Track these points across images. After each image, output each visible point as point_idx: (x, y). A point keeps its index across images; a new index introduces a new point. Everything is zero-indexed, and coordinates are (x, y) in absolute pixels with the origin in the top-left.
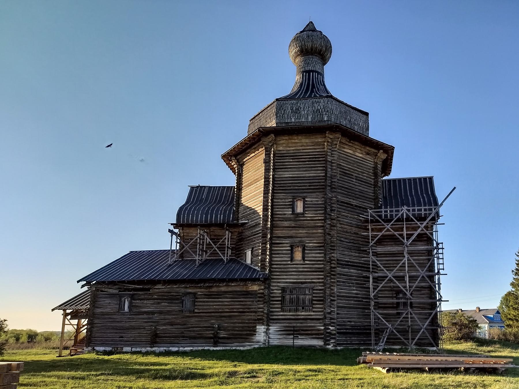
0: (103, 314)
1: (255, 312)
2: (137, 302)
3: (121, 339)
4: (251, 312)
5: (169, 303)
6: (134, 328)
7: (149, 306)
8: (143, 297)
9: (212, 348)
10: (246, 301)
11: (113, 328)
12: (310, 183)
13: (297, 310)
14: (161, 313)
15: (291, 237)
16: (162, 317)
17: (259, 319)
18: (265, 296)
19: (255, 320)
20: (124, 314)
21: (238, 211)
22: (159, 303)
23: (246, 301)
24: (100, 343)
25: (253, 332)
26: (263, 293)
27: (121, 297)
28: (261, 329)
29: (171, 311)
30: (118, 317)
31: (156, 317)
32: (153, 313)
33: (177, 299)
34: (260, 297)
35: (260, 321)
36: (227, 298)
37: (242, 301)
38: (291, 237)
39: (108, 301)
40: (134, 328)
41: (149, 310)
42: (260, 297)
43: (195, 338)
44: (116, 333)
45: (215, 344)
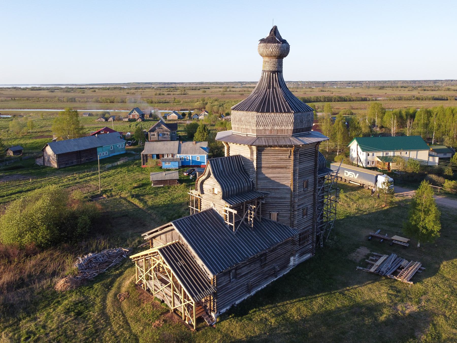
0: (222, 287)
1: (290, 251)
2: (239, 271)
3: (233, 297)
4: (288, 252)
5: (254, 264)
6: (238, 288)
7: (245, 270)
8: (241, 266)
9: (275, 279)
10: (287, 247)
11: (228, 293)
12: (309, 170)
13: (304, 243)
14: (251, 272)
15: (302, 204)
16: (252, 273)
17: (291, 254)
18: (294, 241)
19: (290, 255)
20: (233, 282)
21: (257, 184)
22: (250, 266)
23: (287, 247)
24: (222, 306)
25: (288, 261)
26: (293, 240)
27: (230, 272)
28: (292, 258)
29: (256, 268)
30: (229, 286)
31: (249, 276)
32: (247, 274)
33: (258, 260)
34: (292, 242)
35: (293, 255)
36: (279, 249)
37: (285, 248)
38: (302, 204)
39: (223, 278)
40: (238, 288)
41: (246, 272)
42: (292, 242)
43: (267, 278)
44: (230, 295)
45: (276, 277)
